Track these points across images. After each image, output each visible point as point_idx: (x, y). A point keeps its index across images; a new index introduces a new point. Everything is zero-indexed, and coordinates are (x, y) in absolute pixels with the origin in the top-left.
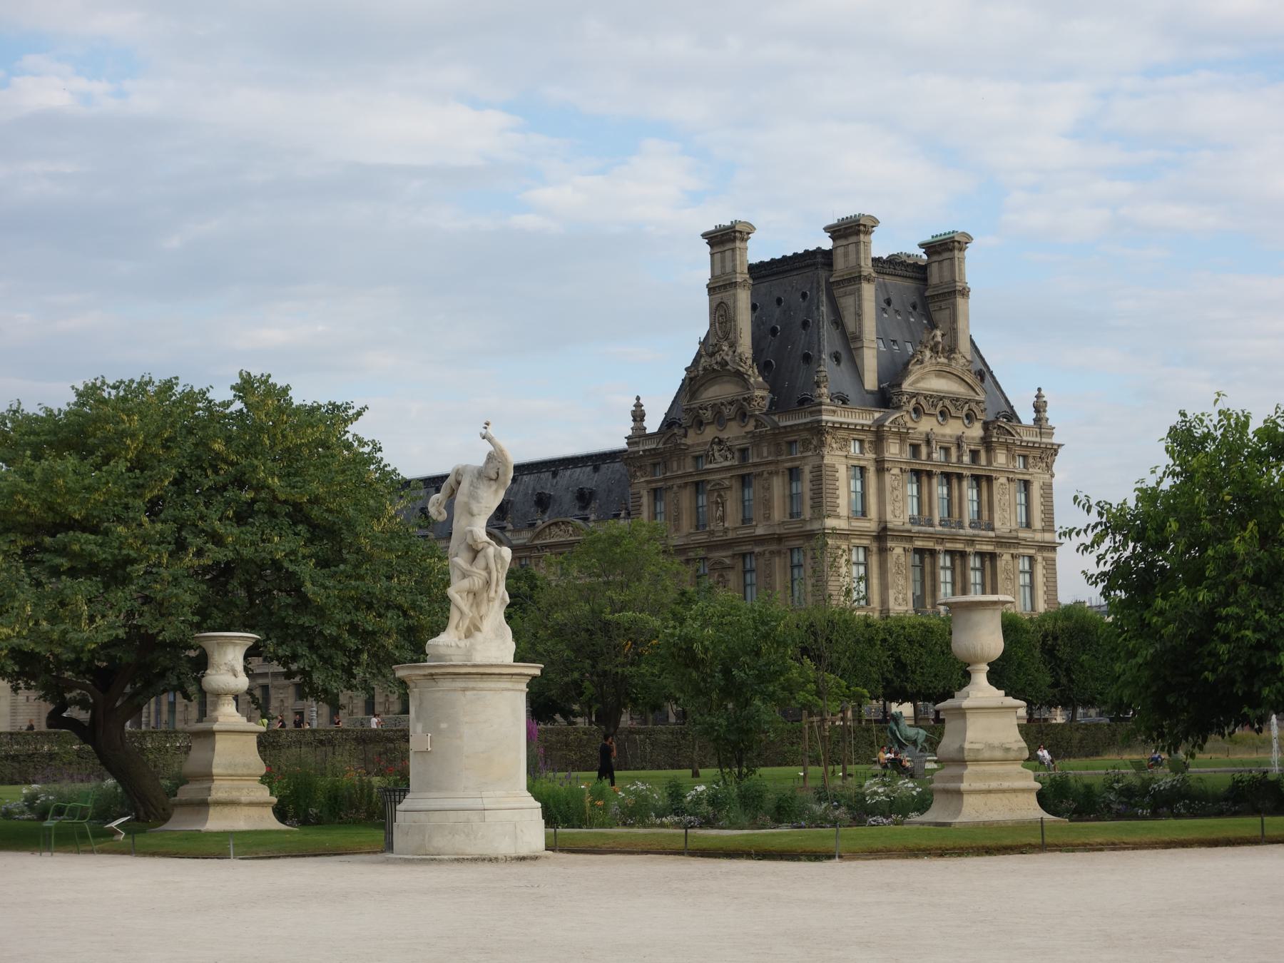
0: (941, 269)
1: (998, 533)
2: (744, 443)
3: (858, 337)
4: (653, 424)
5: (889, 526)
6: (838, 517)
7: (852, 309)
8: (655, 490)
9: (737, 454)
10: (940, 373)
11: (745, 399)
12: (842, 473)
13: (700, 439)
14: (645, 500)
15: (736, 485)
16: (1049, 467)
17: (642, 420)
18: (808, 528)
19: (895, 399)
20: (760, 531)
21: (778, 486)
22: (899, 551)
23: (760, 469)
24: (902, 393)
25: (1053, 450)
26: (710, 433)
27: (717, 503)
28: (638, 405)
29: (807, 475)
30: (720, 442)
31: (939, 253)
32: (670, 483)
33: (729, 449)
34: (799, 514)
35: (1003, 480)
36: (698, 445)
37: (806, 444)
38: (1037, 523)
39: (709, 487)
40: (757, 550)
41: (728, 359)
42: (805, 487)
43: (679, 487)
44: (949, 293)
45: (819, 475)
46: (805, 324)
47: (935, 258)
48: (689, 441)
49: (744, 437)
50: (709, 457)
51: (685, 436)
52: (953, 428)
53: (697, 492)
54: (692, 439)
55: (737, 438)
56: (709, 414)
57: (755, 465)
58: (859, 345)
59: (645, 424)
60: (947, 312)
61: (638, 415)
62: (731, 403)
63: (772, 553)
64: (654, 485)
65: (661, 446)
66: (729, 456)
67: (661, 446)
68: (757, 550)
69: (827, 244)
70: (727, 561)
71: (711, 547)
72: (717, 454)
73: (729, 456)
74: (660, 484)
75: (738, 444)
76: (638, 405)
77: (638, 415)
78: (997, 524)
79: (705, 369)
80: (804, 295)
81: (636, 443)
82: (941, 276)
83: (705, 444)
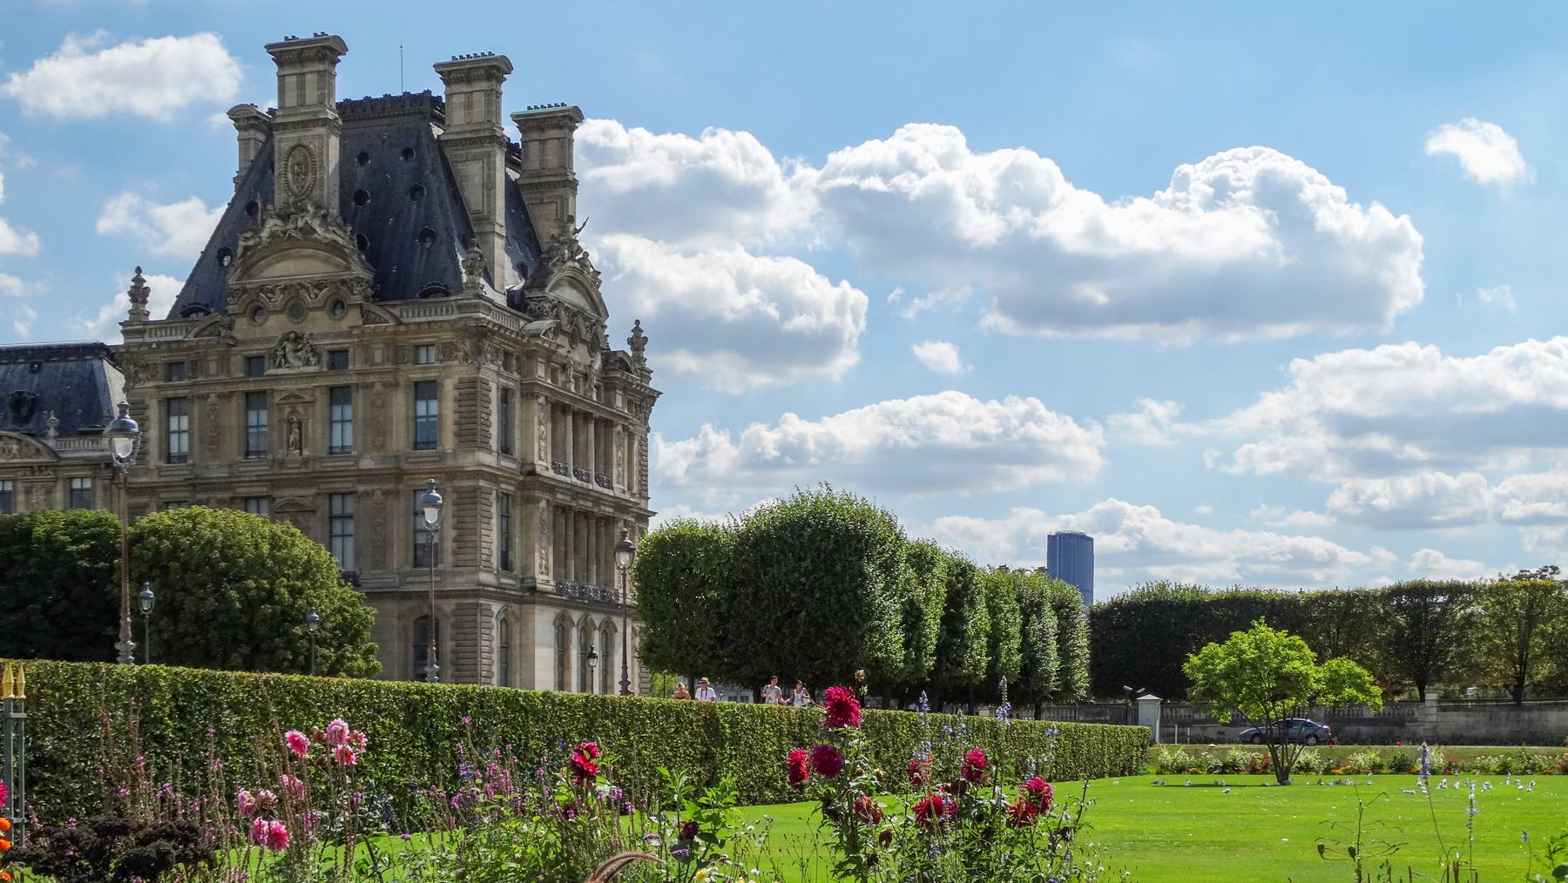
0: (543, 152)
1: (618, 493)
2: (342, 343)
3: (486, 218)
4: (160, 307)
5: (538, 470)
6: (490, 451)
7: (477, 180)
8: (169, 400)
9: (325, 358)
10: (574, 282)
11: (344, 282)
12: (494, 395)
13: (258, 332)
14: (154, 413)
15: (322, 399)
16: (646, 419)
17: (145, 302)
18: (450, 463)
19: (532, 305)
20: (367, 464)
21: (399, 402)
22: (543, 504)
23: (371, 379)
24: (545, 298)
25: (653, 396)
26: (276, 325)
27: (290, 422)
28: (139, 281)
29: (449, 388)
30: (298, 338)
31: (542, 130)
32: (202, 392)
33: (313, 350)
34: (430, 444)
35: (619, 428)
36: (254, 341)
37: (448, 352)
38: (636, 489)
39: (277, 400)
40: (361, 488)
41: (316, 224)
42: (446, 408)
43: (220, 396)
44: (556, 185)
45: (471, 393)
46: (415, 191)
47: (535, 135)
48: (239, 335)
49: (339, 335)
50: (278, 358)
51: (230, 327)
52: (579, 355)
53: (248, 407)
54: (242, 328)
55: (325, 336)
56: (279, 299)
57: (360, 373)
58: (488, 228)
59: (147, 307)
60: (553, 207)
61: (139, 293)
62: (319, 286)
63: (386, 493)
64: (170, 393)
65: (191, 338)
66: (313, 360)
67: (191, 338)
68: (361, 488)
69: (439, 89)
70: (308, 503)
71: (276, 483)
72: (290, 356)
73: (313, 360)
74: (181, 392)
75: (326, 343)
76: (139, 281)
77: (139, 293)
78: (615, 485)
79: (273, 235)
80: (407, 153)
81: (141, 333)
82: (542, 161)
83: (268, 340)
